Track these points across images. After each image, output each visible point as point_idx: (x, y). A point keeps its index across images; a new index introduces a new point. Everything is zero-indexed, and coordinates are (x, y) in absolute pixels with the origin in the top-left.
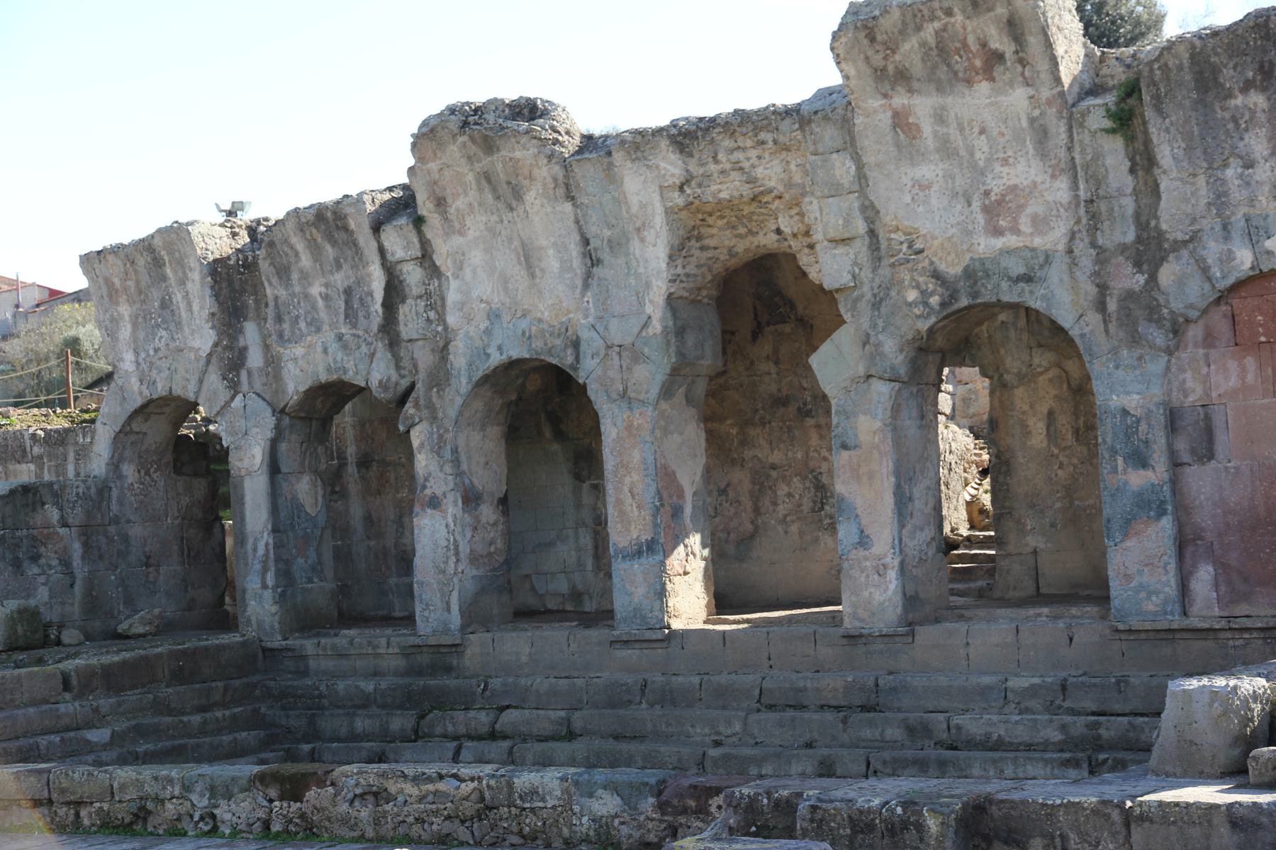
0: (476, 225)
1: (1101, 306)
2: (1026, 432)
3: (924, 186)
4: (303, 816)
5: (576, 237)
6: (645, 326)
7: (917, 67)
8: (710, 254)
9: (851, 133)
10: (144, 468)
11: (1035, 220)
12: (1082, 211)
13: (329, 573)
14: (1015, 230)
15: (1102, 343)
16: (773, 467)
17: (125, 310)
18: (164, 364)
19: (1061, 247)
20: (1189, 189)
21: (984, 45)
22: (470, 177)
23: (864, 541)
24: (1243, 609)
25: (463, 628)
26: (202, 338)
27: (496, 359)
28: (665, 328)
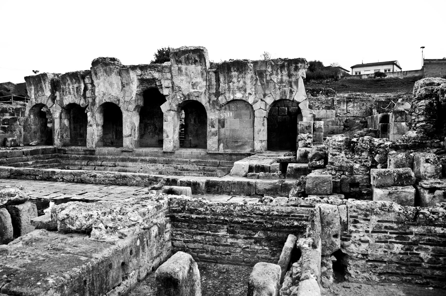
0: (102, 78)
1: (209, 102)
2: (191, 121)
3: (182, 80)
4: (81, 179)
5: (120, 82)
6: (132, 98)
7: (183, 61)
8: (143, 87)
9: (171, 70)
10: (34, 116)
11: (200, 87)
12: (207, 87)
13: (69, 137)
14: (197, 89)
15: (209, 108)
16: (148, 123)
17: (33, 87)
18: (40, 98)
19: (204, 92)
20: (224, 85)
21: (195, 59)
22: (102, 70)
23: (168, 136)
24: (227, 150)
25: (95, 147)
26: (48, 93)
27: (104, 101)
28: (135, 99)
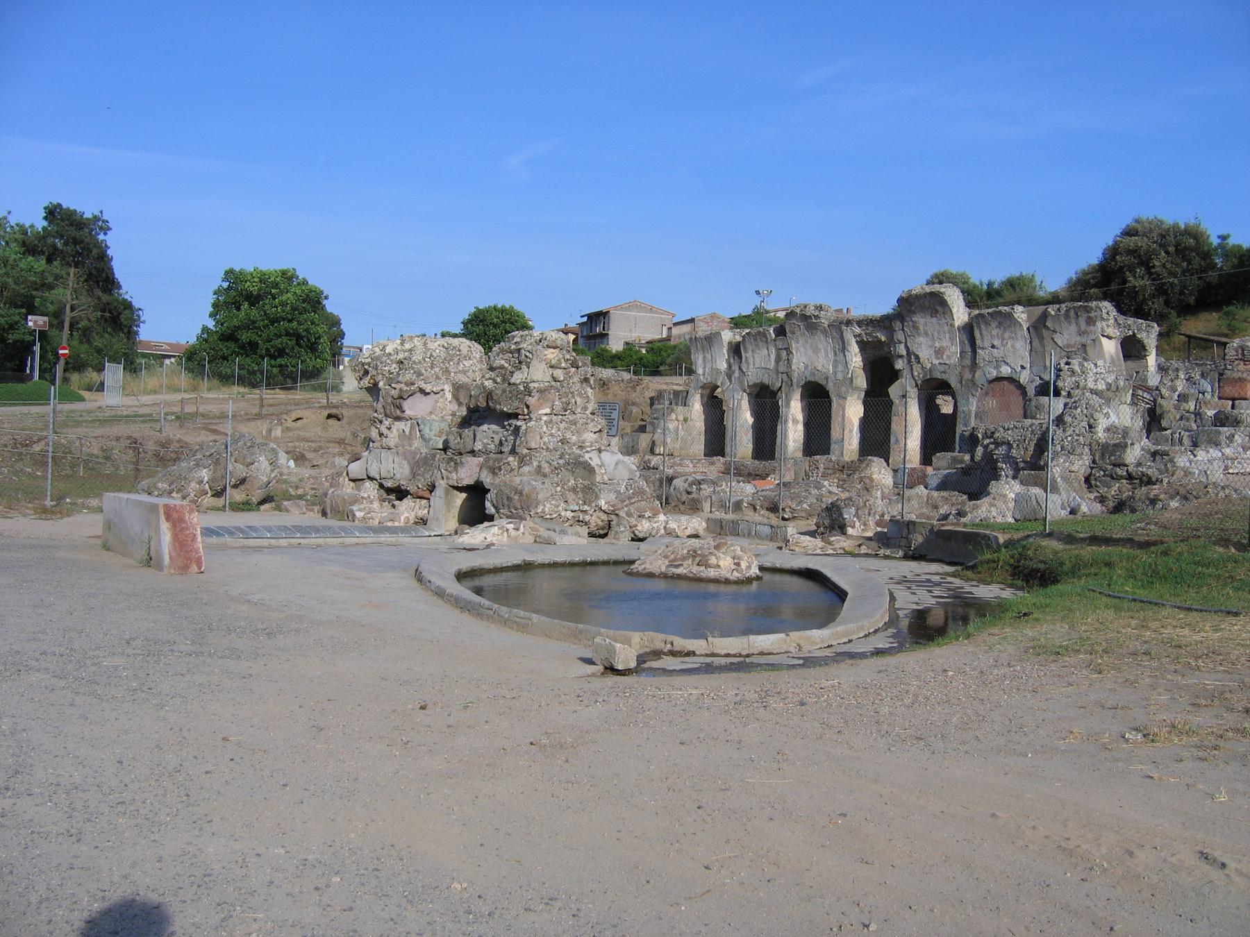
1: (961, 382)
23: (897, 441)
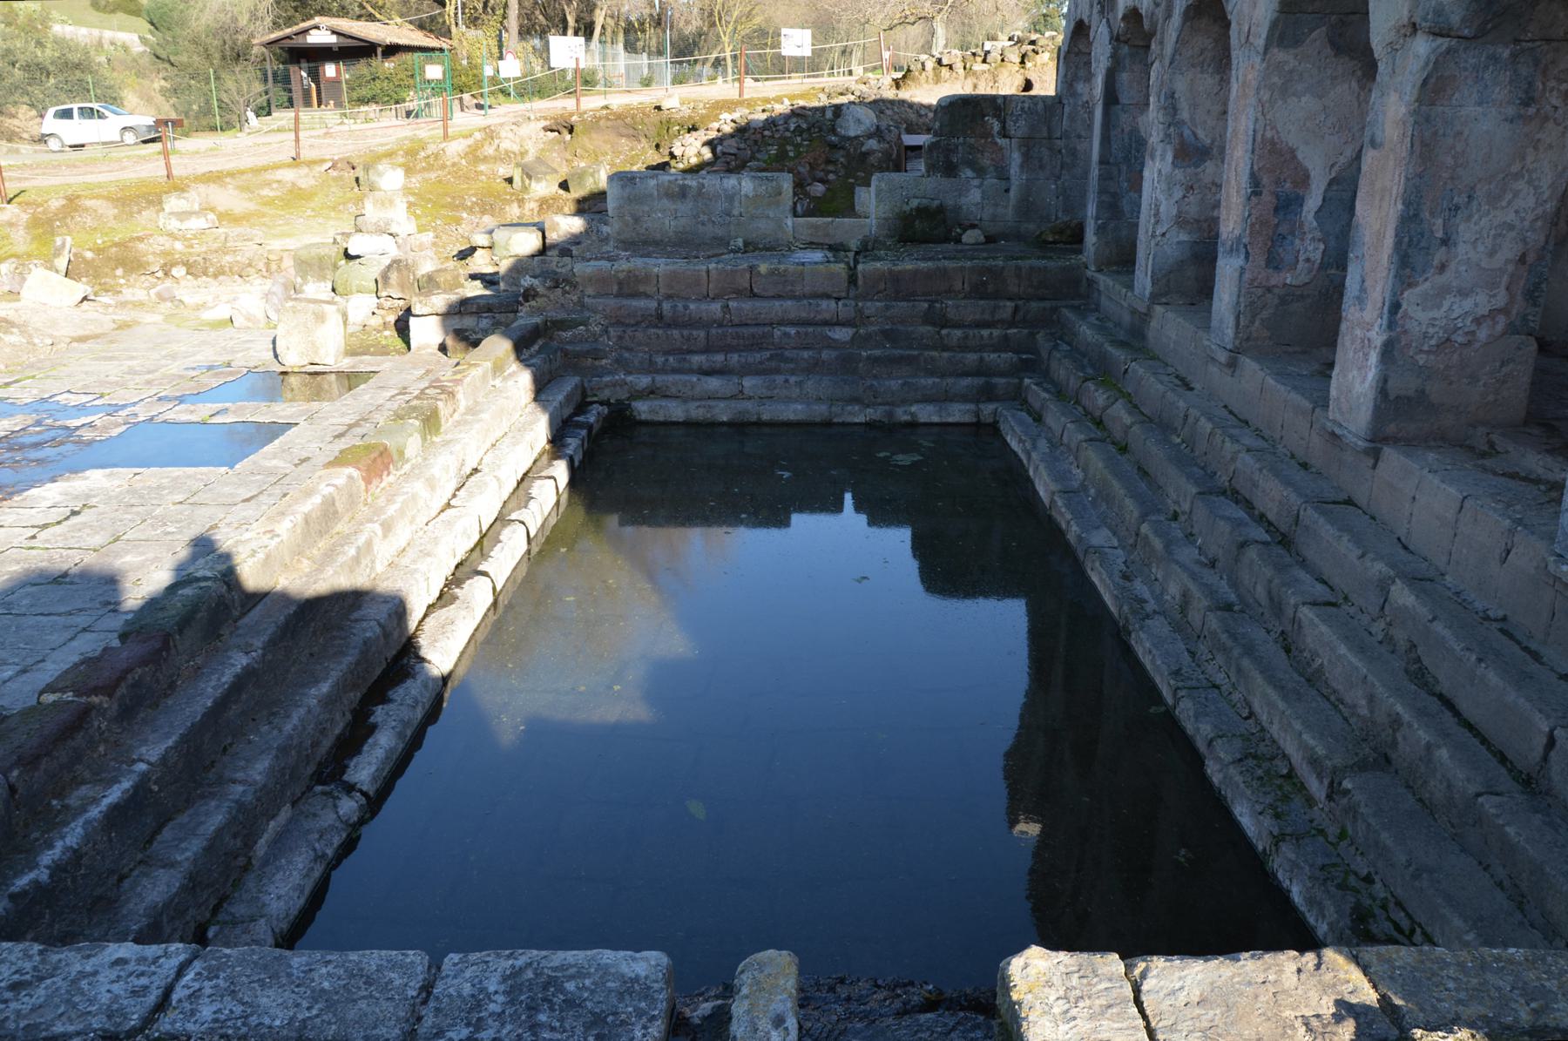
25: (1155, 298)
